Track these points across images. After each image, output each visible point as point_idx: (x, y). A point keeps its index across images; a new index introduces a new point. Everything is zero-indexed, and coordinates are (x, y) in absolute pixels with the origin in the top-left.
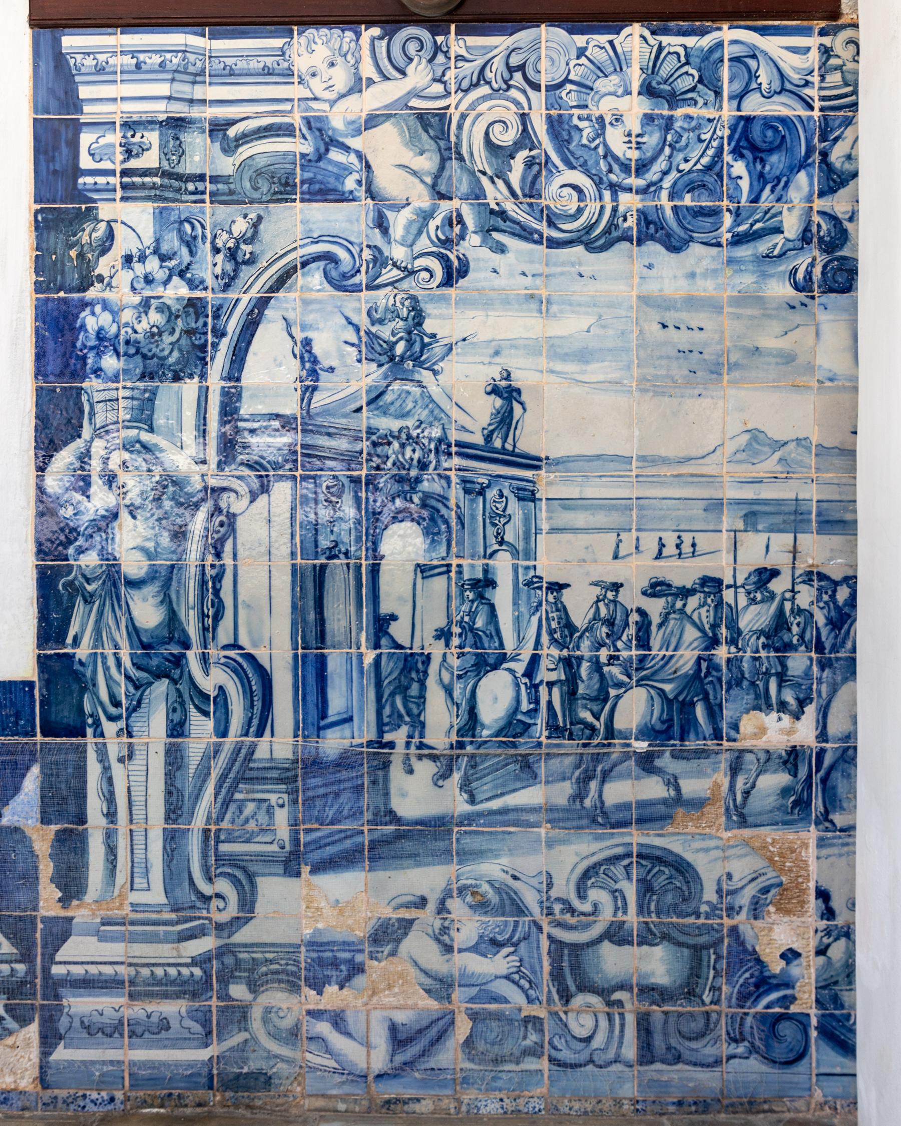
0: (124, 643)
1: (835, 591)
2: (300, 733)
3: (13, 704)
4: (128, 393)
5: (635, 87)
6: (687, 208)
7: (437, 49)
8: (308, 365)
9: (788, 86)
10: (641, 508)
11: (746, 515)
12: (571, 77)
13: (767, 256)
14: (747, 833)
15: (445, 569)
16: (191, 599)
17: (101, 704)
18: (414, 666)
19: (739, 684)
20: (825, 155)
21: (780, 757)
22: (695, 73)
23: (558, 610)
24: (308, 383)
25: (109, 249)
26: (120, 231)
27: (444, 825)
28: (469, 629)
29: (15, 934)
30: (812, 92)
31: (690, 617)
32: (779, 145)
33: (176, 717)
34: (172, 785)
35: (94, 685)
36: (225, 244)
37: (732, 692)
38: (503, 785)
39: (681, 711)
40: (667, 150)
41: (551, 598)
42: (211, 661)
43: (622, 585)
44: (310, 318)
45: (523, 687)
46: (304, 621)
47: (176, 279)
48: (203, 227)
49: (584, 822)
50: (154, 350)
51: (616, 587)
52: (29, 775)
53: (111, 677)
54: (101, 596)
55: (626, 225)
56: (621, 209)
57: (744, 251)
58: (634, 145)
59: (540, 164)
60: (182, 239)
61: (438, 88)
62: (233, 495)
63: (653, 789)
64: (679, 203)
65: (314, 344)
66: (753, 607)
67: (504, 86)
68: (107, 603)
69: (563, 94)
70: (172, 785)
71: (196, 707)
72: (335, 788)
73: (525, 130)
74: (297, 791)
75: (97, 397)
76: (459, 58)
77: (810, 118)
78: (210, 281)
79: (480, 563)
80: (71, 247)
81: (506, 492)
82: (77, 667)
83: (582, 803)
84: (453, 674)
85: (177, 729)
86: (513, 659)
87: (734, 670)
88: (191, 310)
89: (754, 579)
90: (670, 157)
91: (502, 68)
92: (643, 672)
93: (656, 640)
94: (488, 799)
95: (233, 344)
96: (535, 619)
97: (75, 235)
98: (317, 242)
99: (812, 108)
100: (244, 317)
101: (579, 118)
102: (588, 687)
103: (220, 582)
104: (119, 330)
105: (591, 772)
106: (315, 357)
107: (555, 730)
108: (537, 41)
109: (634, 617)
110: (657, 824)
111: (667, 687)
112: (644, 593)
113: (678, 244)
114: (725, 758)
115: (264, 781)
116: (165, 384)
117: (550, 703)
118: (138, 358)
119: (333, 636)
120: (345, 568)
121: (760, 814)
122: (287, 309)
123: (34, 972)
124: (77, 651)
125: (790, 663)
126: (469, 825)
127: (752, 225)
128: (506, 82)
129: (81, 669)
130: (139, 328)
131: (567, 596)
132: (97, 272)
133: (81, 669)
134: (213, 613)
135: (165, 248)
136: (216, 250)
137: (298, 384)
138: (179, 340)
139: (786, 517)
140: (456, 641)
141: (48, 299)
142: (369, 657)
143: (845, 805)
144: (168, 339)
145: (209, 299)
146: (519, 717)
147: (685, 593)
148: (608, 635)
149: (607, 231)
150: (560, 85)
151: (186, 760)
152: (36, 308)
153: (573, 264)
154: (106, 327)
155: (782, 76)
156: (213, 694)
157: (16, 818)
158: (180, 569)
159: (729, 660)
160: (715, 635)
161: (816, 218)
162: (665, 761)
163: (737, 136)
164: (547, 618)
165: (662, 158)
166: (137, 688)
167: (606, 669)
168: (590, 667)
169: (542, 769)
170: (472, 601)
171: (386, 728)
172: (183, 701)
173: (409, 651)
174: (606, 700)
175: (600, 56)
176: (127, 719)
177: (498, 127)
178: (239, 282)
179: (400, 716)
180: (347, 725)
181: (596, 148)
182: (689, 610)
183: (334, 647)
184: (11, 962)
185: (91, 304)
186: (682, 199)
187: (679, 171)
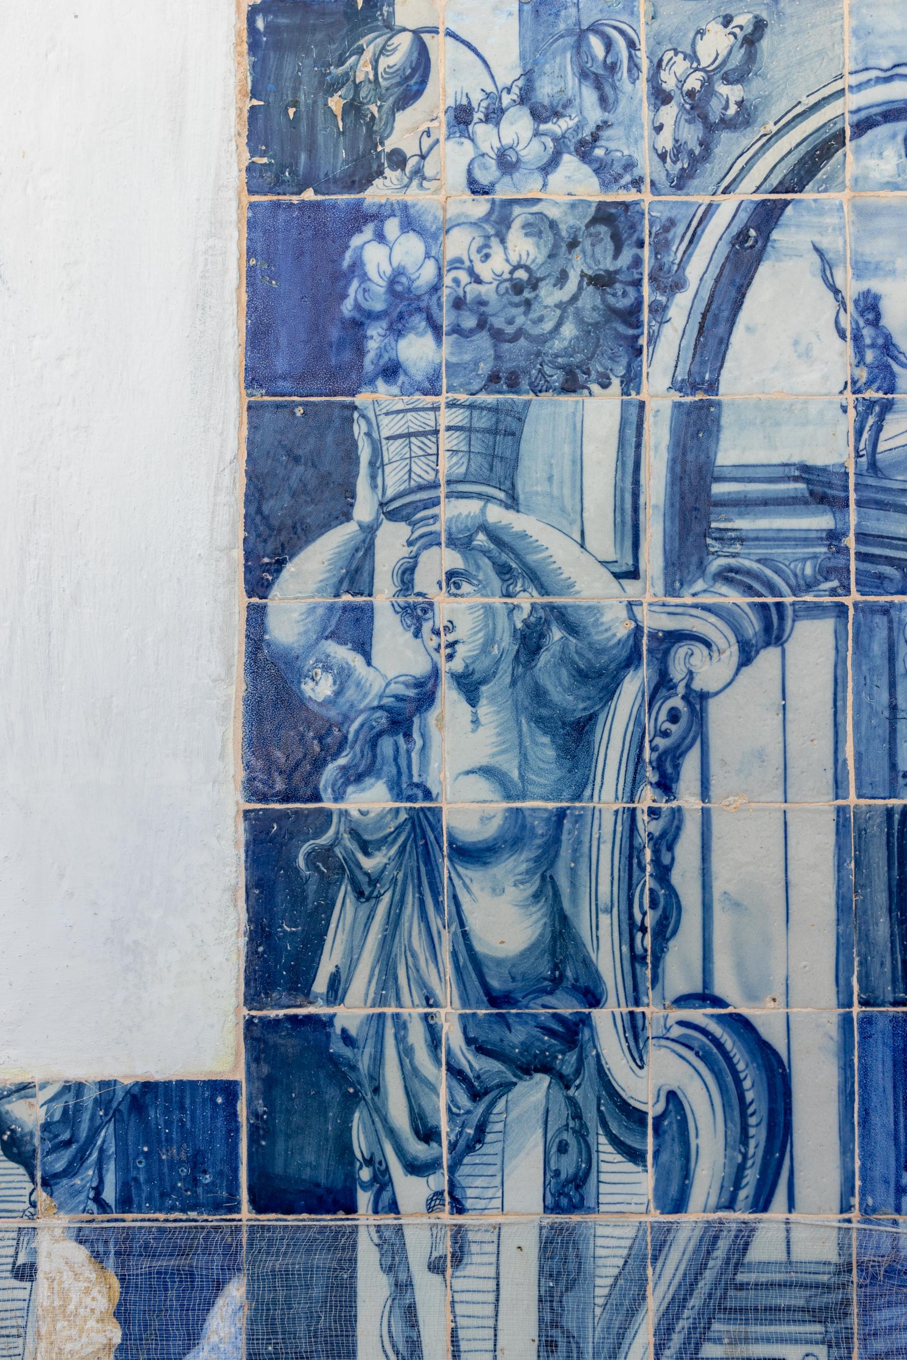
0: (447, 991)
2: (856, 1201)
4: (458, 417)
8: (870, 356)
16: (604, 888)
17: (392, 1133)
25: (418, 94)
26: (441, 51)
33: (568, 1165)
34: (555, 1324)
35: (376, 1090)
36: (681, 82)
42: (650, 1033)
44: (877, 249)
46: (865, 938)
47: (569, 162)
48: (632, 45)
50: (520, 320)
53: (415, 1071)
54: (394, 881)
62: (699, 650)
65: (885, 306)
68: (409, 899)
70: (555, 1324)
71: (615, 1141)
74: (849, 1339)
75: (389, 426)
78: (647, 166)
80: (332, 88)
82: (337, 1047)
85: (569, 1192)
88: (603, 229)
95: (701, 307)
97: (341, 62)
98: (888, 80)
100: (724, 249)
103: (670, 848)
104: (440, 276)
106: (888, 338)
115: (772, 1313)
116: (545, 397)
118: (483, 340)
122: (822, 230)
129: (347, 1052)
130: (484, 270)
132: (390, 145)
133: (347, 1052)
135: (545, 91)
136: (661, 97)
137: (849, 398)
138: (574, 298)
141: (277, 205)
145: (645, 206)
151: (588, 1266)
152: (252, 225)
154: (411, 269)
156: (652, 1111)
158: (579, 819)
166: (475, 1096)
172: (583, 1126)
176: (452, 1170)
178: (713, 170)
185: (377, 217)
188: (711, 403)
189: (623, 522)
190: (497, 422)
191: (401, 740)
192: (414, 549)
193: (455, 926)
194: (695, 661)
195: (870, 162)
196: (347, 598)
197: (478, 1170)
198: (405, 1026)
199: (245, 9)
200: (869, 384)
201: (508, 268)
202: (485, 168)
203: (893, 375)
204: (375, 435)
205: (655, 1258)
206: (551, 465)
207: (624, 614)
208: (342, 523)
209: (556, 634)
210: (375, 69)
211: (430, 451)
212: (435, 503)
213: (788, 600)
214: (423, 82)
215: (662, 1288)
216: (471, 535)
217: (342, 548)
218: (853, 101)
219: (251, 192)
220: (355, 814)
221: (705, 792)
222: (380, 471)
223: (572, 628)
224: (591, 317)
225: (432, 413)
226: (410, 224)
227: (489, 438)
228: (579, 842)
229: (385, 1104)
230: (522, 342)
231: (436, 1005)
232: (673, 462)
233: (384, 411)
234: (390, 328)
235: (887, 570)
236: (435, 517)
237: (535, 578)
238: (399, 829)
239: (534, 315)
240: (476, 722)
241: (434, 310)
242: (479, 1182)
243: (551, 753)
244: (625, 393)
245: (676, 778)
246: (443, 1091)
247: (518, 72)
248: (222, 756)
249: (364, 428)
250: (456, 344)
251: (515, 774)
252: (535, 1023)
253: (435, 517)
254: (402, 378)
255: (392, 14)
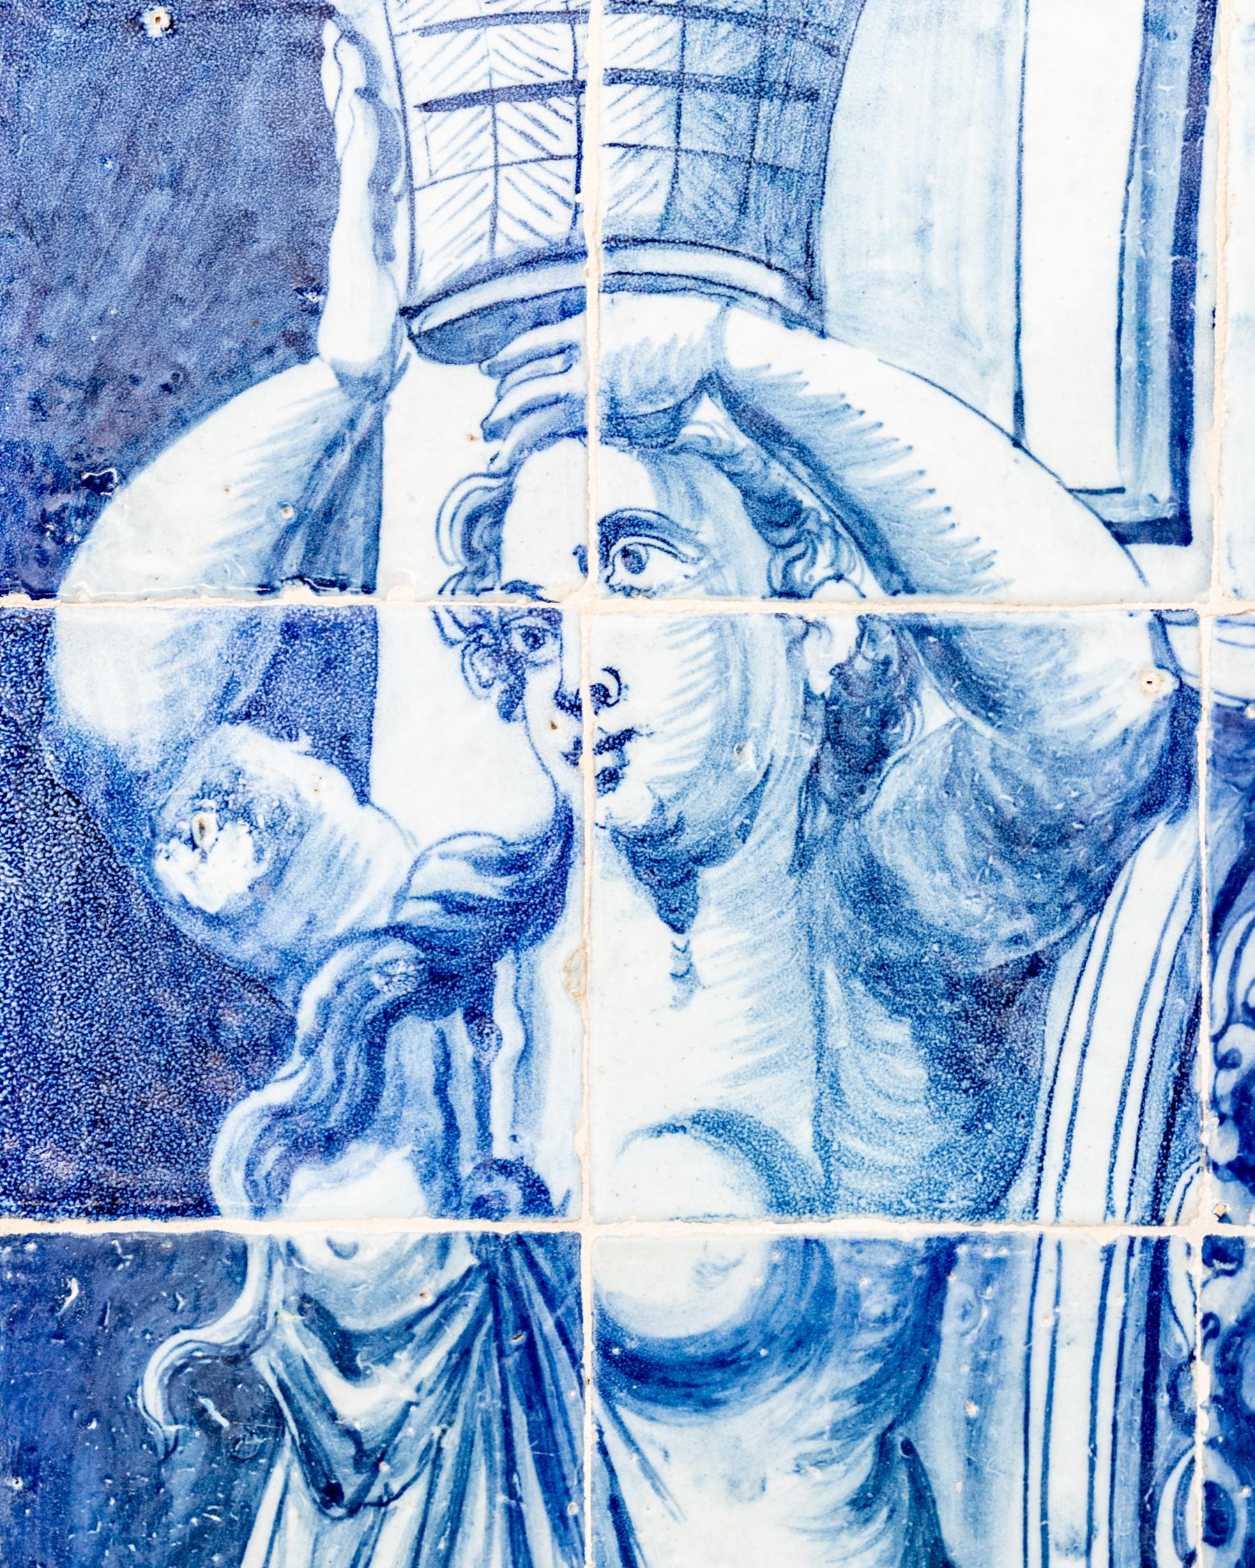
189: (1144, 370)
190: (762, 60)
192: (504, 448)
204: (389, 96)
206: (926, 192)
208: (283, 367)
211: (557, 149)
212: (570, 309)
216: (679, 407)
217: (284, 444)
222: (403, 206)
225: (562, 29)
233: (418, 22)
249: (356, 77)
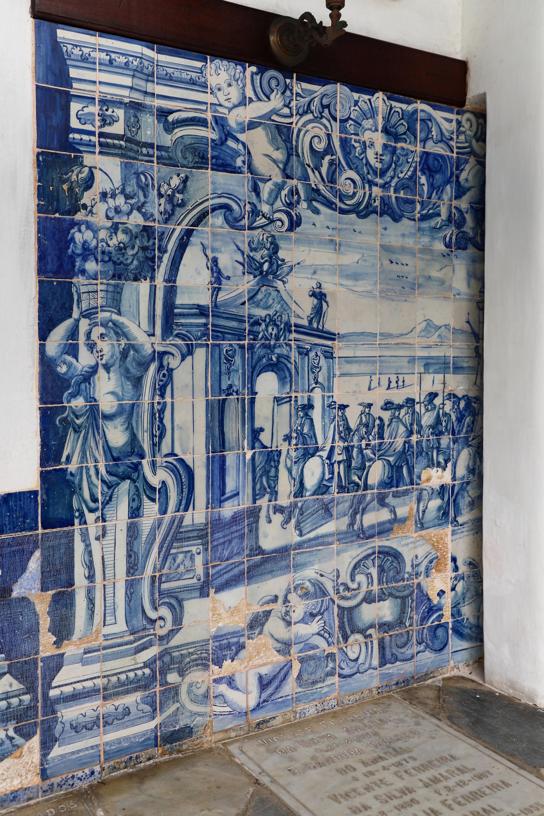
0: (101, 457)
1: (459, 403)
2: (210, 506)
3: (21, 508)
4: (103, 287)
5: (380, 128)
6: (402, 198)
7: (286, 87)
8: (215, 275)
9: (444, 139)
10: (381, 362)
11: (425, 365)
12: (352, 116)
13: (434, 228)
14: (424, 532)
15: (288, 399)
16: (145, 425)
17: (85, 501)
18: (272, 458)
19: (421, 455)
20: (458, 177)
21: (437, 491)
22: (405, 124)
23: (343, 420)
24: (215, 285)
26: (98, 175)
27: (287, 551)
28: (300, 434)
29: (22, 675)
30: (453, 143)
31: (401, 420)
32: (440, 170)
33: (135, 505)
34: (131, 550)
35: (80, 489)
36: (166, 192)
37: (418, 459)
38: (316, 523)
39: (397, 471)
40: (393, 165)
41: (340, 414)
42: (158, 465)
43: (372, 405)
44: (217, 244)
45: (326, 465)
46: (213, 435)
47: (135, 212)
48: (152, 179)
49: (354, 538)
50: (121, 259)
51: (370, 405)
52: (32, 558)
53: (92, 482)
54: (86, 426)
55: (375, 204)
56: (373, 195)
57: (425, 225)
58: (379, 160)
59: (336, 164)
60: (139, 186)
61: (286, 111)
62: (171, 356)
63: (385, 515)
64: (398, 195)
65: (220, 261)
66: (427, 413)
67: (320, 116)
68: (90, 431)
69: (348, 126)
70: (131, 550)
71: (148, 497)
72: (229, 537)
73: (329, 143)
74: (208, 543)
75: (83, 289)
76: (298, 94)
77: (452, 157)
78: (157, 216)
79: (306, 395)
80: (64, 182)
81: (319, 354)
82: (69, 477)
83: (353, 527)
84: (292, 461)
85: (135, 512)
86: (322, 450)
87: (420, 447)
88: (145, 234)
89: (428, 398)
90: (395, 169)
91: (319, 105)
92: (380, 451)
93: (386, 435)
94: (308, 533)
95: (171, 258)
96: (332, 426)
97: (66, 174)
98: (220, 197)
99: (453, 152)
100: (177, 242)
101: (355, 141)
102: (356, 462)
103: (163, 413)
105: (358, 509)
106: (220, 270)
107: (341, 488)
108: (335, 92)
109: (377, 422)
110: (386, 535)
111: (391, 459)
112: (382, 409)
113: (397, 218)
114: (415, 493)
115: (189, 539)
116: (128, 282)
117: (339, 473)
118: (110, 264)
119: (229, 443)
120: (236, 401)
121: (429, 522)
122: (203, 238)
123: (37, 698)
124: (69, 466)
125: (442, 442)
126: (299, 549)
127: (428, 211)
128: (321, 113)
129: (72, 478)
130: (111, 243)
131: (348, 412)
132: (82, 202)
133: (72, 478)
134: (159, 434)
135: (128, 190)
136: (160, 195)
137: (210, 286)
138: (137, 253)
139: (440, 366)
140: (294, 442)
141: (47, 218)
142: (249, 455)
143: (462, 512)
144: (130, 252)
146: (325, 483)
147: (399, 407)
148: (366, 433)
149: (367, 207)
150: (346, 120)
151: (140, 533)
152: (39, 223)
153: (351, 224)
154: (89, 241)
155: (442, 133)
156: (158, 487)
157: (23, 590)
158: (138, 406)
159: (417, 442)
160: (411, 429)
161: (454, 210)
162: (390, 500)
163: (423, 162)
164: (338, 425)
165: (391, 169)
166: (109, 488)
167: (365, 451)
168: (357, 451)
169: (335, 512)
170: (302, 418)
171: (257, 497)
172: (139, 493)
173: (270, 449)
174: (364, 469)
175: (365, 107)
176: (102, 510)
177: (316, 140)
178: (175, 218)
179: (265, 489)
180: (236, 498)
181: (362, 159)
182: (401, 416)
183: (230, 450)
184: (20, 695)
185: (78, 224)
186: (400, 193)
187: (399, 178)
188: (174, 286)
191: (87, 384)
193: (103, 439)
194: (170, 359)
195: (216, 220)
196: (71, 341)
197: (110, 509)
198: (89, 469)
199: (36, 153)
200: (215, 282)
201: (117, 243)
202: (111, 212)
203: (221, 281)
205: (158, 528)
207: (150, 346)
209: (132, 352)
210: (77, 177)
212: (97, 313)
213: (194, 342)
214: (93, 183)
215: (160, 536)
218: (211, 202)
219: (39, 213)
220: (74, 407)
221: (172, 397)
223: (136, 351)
224: (141, 259)
226: (89, 226)
227: (112, 294)
228: (138, 412)
229: (83, 493)
230: (122, 265)
231: (98, 462)
232: (164, 303)
234: (83, 259)
235: (219, 334)
236: (97, 317)
237: (126, 335)
238: (87, 411)
239: (126, 257)
240: (109, 378)
241: (96, 254)
242: (110, 512)
243: (130, 387)
244: (151, 282)
245: (165, 393)
246: (100, 487)
247: (120, 184)
248: (32, 391)
250: (102, 265)
251: (120, 393)
252: (125, 465)
253: (97, 317)
254: (86, 274)
255: (83, 161)
